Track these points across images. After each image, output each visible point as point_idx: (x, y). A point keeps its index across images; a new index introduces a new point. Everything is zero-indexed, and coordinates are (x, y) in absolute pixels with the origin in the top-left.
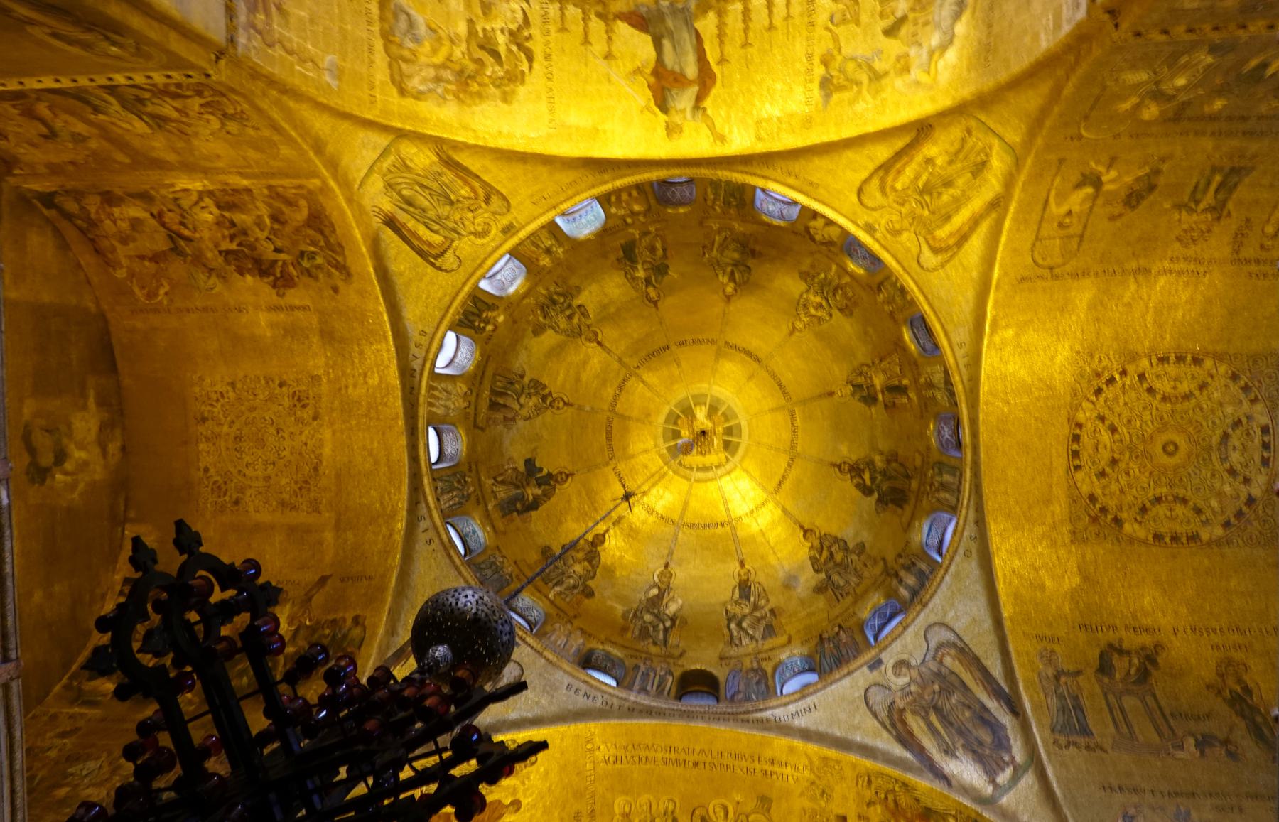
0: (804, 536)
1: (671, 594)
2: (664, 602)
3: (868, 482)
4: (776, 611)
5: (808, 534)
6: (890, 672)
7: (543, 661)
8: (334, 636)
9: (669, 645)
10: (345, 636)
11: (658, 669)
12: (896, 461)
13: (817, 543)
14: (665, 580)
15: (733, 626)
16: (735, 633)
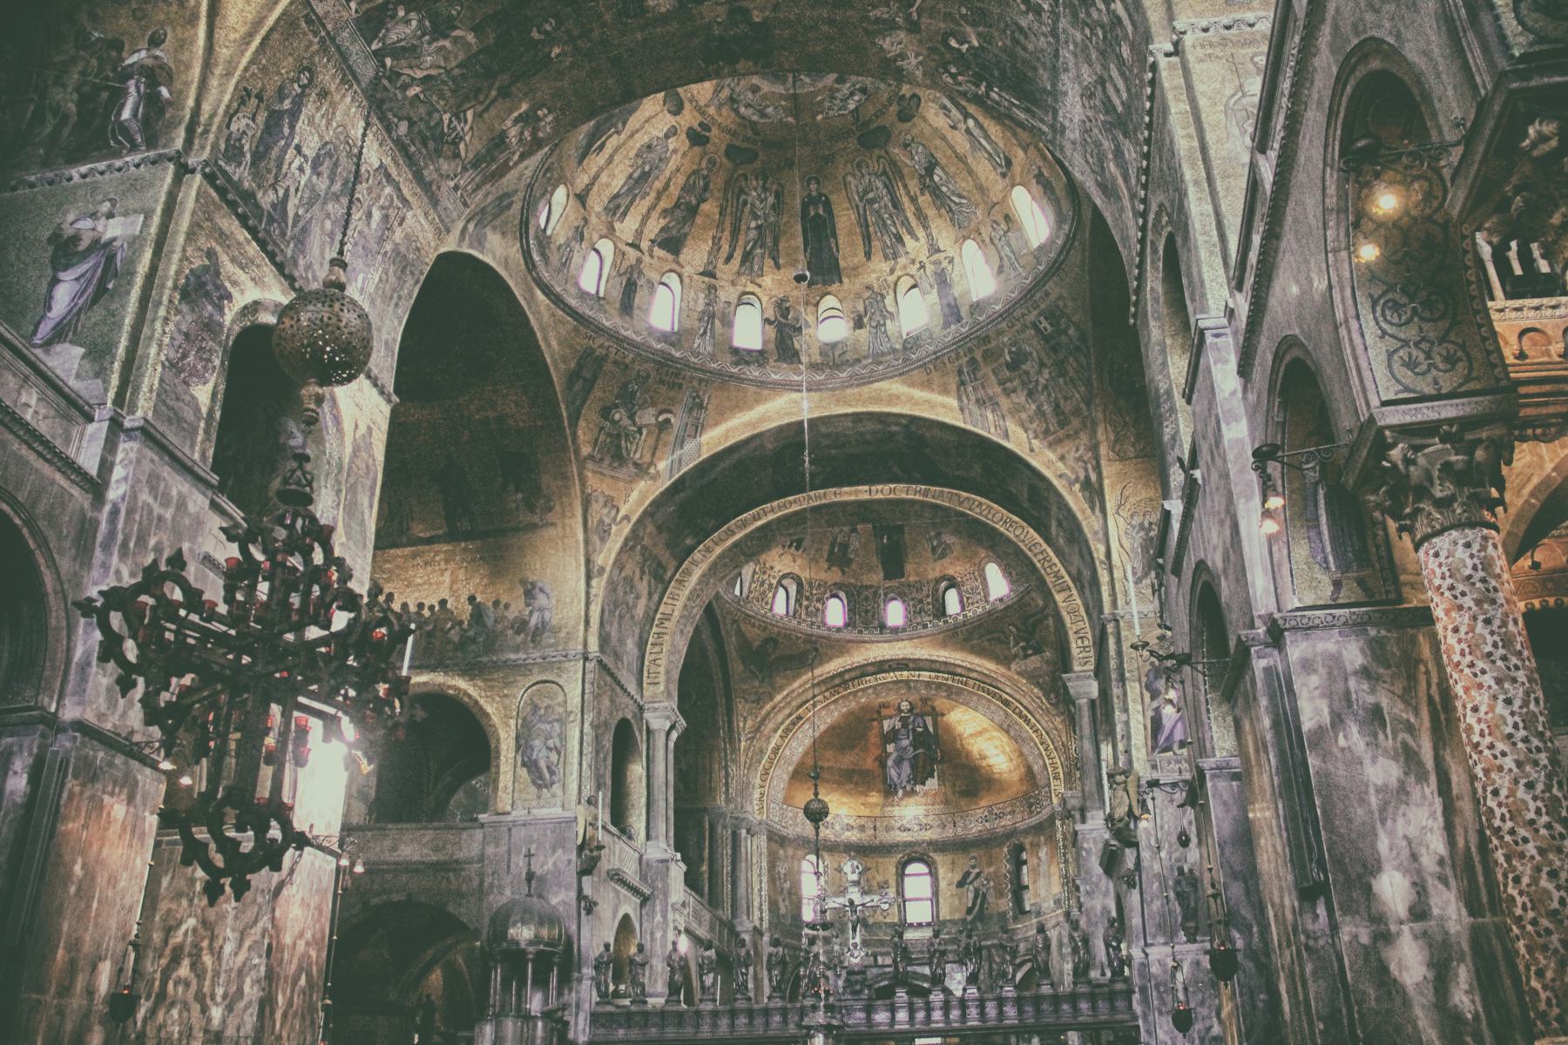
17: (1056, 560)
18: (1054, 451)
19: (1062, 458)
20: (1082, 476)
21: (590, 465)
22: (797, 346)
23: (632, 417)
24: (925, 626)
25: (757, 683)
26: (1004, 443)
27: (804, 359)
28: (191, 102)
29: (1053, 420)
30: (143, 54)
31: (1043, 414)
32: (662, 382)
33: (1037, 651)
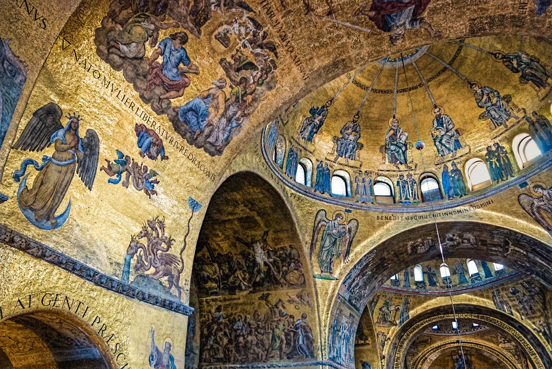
0: (471, 87)
1: (401, 132)
2: (398, 137)
3: (515, 66)
4: (458, 130)
5: (474, 86)
6: (532, 190)
7: (363, 211)
8: (286, 254)
9: (408, 163)
10: (290, 254)
11: (408, 180)
12: (538, 62)
13: (479, 91)
14: (395, 124)
15: (437, 143)
16: (440, 148)
17: (528, 343)
18: (531, 320)
19: (534, 323)
20: (543, 330)
21: (377, 324)
22: (435, 280)
23: (388, 309)
24: (467, 331)
25: (412, 350)
26: (512, 316)
27: (438, 284)
28: (319, 341)
29: (530, 312)
30: (301, 321)
31: (526, 309)
32: (396, 298)
33: (509, 342)
